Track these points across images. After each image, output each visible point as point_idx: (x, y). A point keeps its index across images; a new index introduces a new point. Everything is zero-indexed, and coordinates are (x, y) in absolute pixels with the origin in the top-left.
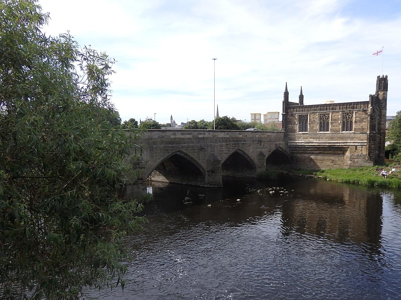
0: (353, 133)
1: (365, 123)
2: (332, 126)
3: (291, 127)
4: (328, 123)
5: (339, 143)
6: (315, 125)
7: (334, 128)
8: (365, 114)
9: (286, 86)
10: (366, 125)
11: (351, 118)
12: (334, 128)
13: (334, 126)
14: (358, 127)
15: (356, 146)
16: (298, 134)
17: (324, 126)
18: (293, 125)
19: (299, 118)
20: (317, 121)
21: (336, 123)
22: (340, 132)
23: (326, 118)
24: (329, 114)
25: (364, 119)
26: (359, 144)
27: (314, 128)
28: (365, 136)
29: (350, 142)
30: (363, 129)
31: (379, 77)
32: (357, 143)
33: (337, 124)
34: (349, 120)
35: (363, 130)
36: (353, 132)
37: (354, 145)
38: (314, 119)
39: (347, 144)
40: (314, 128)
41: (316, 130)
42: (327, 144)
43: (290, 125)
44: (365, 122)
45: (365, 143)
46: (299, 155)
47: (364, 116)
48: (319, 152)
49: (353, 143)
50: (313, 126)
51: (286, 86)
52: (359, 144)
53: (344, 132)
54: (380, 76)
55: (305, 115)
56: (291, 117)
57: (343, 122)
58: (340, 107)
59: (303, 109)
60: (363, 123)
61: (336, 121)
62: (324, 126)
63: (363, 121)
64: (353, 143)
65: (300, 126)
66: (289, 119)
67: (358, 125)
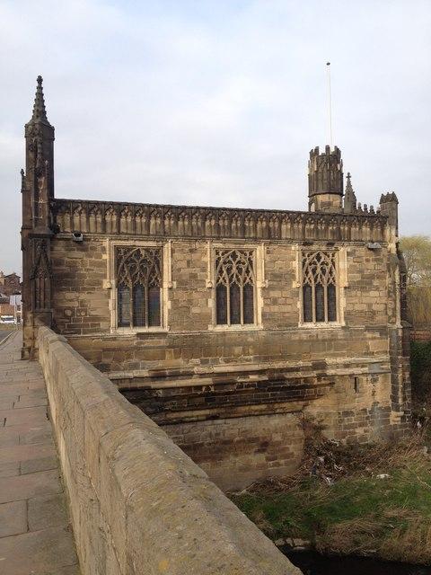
0: (343, 328)
1: (376, 293)
2: (268, 302)
3: (76, 304)
4: (249, 289)
5: (297, 370)
6: (195, 295)
7: (275, 309)
8: (375, 260)
9: (40, 88)
10: (377, 299)
11: (331, 272)
12: (275, 309)
13: (275, 302)
14: (357, 307)
15: (355, 380)
16: (114, 339)
18: (83, 296)
19: (118, 260)
20: (210, 282)
21: (282, 289)
22: (300, 326)
23: (240, 270)
24: (251, 254)
25: (372, 277)
26: (366, 370)
27: (195, 310)
28: (385, 344)
29: (335, 363)
30: (374, 313)
31: (314, 153)
32: (357, 365)
33: (285, 294)
34: (325, 281)
35: (372, 318)
36: (344, 324)
37: (351, 376)
38: (185, 271)
39: (330, 372)
40: (195, 310)
41: (204, 319)
42: (253, 378)
43: (69, 295)
44: (377, 289)
45: (382, 363)
47: (371, 267)
48: (207, 412)
49: (347, 366)
50: (190, 301)
51: (40, 96)
52: (366, 370)
53: (309, 325)
54: (317, 149)
55: (147, 250)
56: (77, 254)
57: (306, 287)
58: (295, 226)
59: (138, 220)
60: (373, 293)
61: (283, 283)
62: (233, 301)
63: (371, 283)
64: (347, 366)
65: (120, 297)
66: (59, 263)
67: (357, 301)
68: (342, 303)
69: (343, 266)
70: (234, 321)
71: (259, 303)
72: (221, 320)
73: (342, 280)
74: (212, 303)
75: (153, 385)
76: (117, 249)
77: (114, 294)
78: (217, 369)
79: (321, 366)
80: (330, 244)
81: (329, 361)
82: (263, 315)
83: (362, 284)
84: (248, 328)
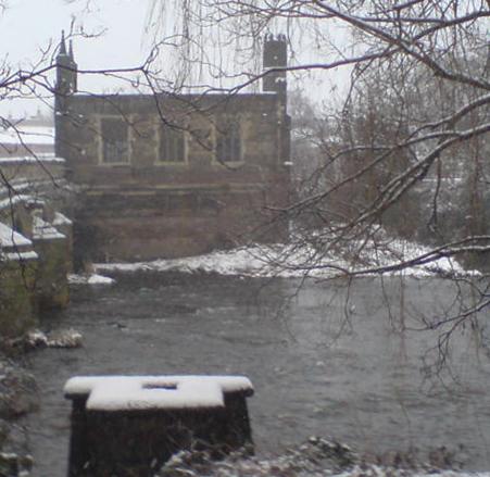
17: (171, 149)
27: (146, 154)
39: (233, 191)
46: (100, 223)
60: (265, 144)
62: (171, 149)
64: (244, 188)
68: (244, 150)
69: (246, 127)
70: (172, 160)
71: (187, 149)
72: (163, 159)
73: (244, 135)
74: (156, 149)
75: (122, 193)
76: (103, 120)
77: (101, 144)
78: (158, 187)
79: (226, 188)
80: (235, 113)
81: (232, 184)
82: (189, 157)
83: (256, 137)
84: (182, 164)
